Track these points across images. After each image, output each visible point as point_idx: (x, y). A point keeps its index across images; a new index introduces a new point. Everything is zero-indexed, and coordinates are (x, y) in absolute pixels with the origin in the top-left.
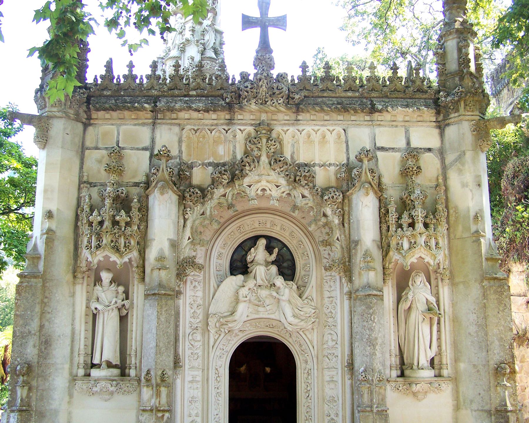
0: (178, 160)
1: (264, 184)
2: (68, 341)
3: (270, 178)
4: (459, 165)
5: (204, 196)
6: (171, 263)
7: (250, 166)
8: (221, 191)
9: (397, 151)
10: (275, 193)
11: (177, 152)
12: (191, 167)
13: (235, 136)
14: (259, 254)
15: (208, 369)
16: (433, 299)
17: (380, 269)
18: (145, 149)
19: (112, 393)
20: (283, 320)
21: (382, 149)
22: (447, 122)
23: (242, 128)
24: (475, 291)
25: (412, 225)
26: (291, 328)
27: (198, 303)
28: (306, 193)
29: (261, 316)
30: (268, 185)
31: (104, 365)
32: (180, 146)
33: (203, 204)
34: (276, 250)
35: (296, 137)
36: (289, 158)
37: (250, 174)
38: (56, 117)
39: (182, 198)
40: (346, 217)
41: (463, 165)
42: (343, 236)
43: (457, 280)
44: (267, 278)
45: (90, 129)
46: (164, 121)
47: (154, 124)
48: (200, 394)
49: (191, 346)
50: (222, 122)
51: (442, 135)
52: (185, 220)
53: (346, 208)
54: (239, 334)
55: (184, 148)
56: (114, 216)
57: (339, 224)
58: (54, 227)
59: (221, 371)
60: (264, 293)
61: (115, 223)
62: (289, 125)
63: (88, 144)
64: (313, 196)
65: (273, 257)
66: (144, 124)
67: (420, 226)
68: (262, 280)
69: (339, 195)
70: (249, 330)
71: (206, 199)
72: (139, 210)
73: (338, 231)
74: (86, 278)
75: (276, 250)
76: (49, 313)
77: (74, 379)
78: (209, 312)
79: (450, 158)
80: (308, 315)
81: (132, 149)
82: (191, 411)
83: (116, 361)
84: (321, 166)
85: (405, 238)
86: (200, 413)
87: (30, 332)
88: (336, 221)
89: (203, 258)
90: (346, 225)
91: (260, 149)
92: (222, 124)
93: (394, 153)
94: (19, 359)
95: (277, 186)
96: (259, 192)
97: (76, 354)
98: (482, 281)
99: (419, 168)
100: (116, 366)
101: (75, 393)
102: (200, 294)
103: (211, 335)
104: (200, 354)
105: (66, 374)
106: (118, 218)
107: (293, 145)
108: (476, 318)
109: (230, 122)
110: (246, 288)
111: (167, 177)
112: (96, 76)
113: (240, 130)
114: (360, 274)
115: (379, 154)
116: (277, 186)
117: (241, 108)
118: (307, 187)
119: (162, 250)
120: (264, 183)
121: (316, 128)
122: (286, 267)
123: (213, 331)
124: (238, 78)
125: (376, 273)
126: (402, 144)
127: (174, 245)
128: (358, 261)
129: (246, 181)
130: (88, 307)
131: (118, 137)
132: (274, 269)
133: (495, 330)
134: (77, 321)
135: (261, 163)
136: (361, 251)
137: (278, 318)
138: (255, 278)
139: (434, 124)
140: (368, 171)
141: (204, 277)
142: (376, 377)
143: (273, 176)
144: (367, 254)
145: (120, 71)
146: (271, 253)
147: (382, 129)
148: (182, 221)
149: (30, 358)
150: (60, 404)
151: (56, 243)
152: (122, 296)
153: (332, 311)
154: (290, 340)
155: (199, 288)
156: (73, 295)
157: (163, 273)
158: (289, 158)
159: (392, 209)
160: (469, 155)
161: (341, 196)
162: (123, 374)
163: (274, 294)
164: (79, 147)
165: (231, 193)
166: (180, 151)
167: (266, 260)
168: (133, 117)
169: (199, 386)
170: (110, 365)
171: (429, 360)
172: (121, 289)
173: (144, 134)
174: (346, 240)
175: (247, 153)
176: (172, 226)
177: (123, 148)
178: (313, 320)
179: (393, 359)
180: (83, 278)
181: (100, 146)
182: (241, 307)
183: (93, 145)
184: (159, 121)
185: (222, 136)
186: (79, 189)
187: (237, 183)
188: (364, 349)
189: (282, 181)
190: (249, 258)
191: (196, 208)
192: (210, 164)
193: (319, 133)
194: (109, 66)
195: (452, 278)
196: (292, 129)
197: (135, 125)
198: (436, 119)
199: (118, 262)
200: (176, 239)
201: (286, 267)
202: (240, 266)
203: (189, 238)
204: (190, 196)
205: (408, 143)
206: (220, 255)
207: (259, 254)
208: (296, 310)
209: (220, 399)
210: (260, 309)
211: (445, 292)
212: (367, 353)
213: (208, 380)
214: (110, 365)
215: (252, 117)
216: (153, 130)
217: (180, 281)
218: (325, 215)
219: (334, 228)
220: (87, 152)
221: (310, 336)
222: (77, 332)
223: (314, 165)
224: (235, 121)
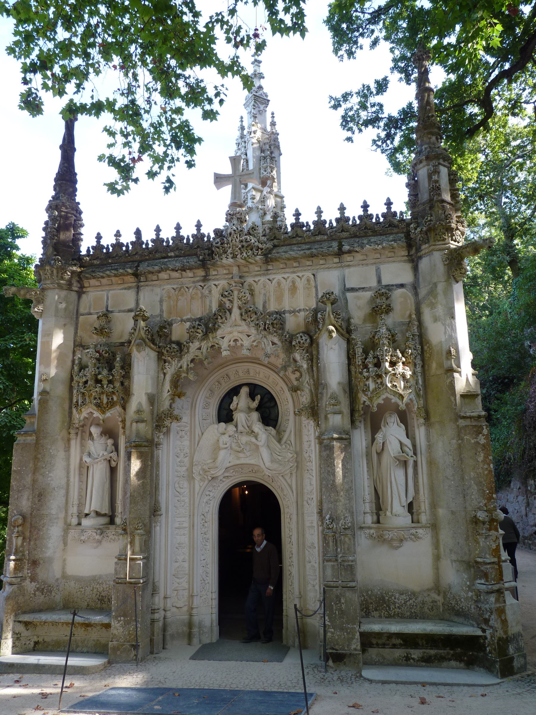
0: (159, 319)
1: (236, 335)
2: (63, 492)
3: (240, 329)
4: (431, 298)
5: (181, 350)
6: (146, 416)
7: (222, 318)
8: (197, 344)
9: (367, 291)
10: (247, 342)
11: (159, 311)
12: (170, 324)
13: (210, 291)
14: (242, 401)
15: (194, 515)
16: (407, 442)
17: (346, 411)
18: (130, 311)
19: (100, 542)
21: (352, 290)
22: (419, 254)
23: (217, 283)
24: (450, 430)
28: (276, 340)
29: (242, 461)
30: (240, 335)
31: (93, 514)
32: (161, 305)
33: (181, 358)
34: (259, 397)
35: (267, 286)
36: (261, 308)
37: (222, 326)
38: (50, 289)
39: (160, 355)
40: (315, 361)
41: (435, 297)
42: (311, 380)
43: (433, 420)
45: (84, 296)
46: (147, 283)
47: (138, 287)
48: (187, 540)
49: (177, 494)
50: (198, 278)
51: (416, 269)
52: (165, 374)
53: (314, 353)
54: (224, 480)
55: (165, 308)
56: (96, 375)
57: (308, 369)
58: (48, 389)
59: (209, 517)
60: (244, 439)
61: (98, 381)
62: (260, 275)
63: (82, 310)
64: (282, 342)
65: (255, 404)
66: (129, 288)
69: (306, 340)
71: (183, 353)
72: (122, 368)
73: (307, 376)
74: (80, 433)
76: (43, 467)
77: (67, 527)
79: (423, 291)
81: (120, 311)
82: (178, 557)
83: (105, 510)
84: (290, 312)
85: (370, 379)
86: (187, 558)
87: (25, 486)
88: (305, 366)
90: (315, 369)
91: (231, 301)
92: (198, 281)
93: (364, 293)
94: (15, 512)
95: (249, 336)
96: (232, 343)
97: (70, 505)
98: (456, 421)
99: (389, 306)
100: (105, 515)
101: (69, 541)
102: (187, 443)
103: (196, 482)
104: (187, 500)
105: (61, 524)
106: (99, 377)
107: (265, 295)
108: (452, 461)
109: (205, 279)
110: (226, 436)
111: (144, 336)
112: (89, 248)
113: (215, 285)
114: (326, 418)
115: (349, 295)
116: (249, 336)
117: (214, 265)
118: (275, 334)
119: (140, 404)
120: (235, 333)
121: (286, 276)
122: (268, 412)
123: (197, 478)
124: (212, 235)
125: (343, 417)
126: (374, 283)
127: (152, 399)
128: (324, 405)
129: (219, 333)
130: (81, 459)
131: (107, 302)
132: (255, 415)
133: (472, 473)
134: (72, 473)
135: (232, 314)
136: (327, 394)
138: (236, 426)
139: (406, 258)
140: (331, 313)
141: (191, 428)
142: (340, 525)
143: (244, 327)
144: (334, 397)
145: (108, 240)
146: (253, 400)
147: (352, 269)
148: (162, 375)
149: (25, 510)
150: (55, 552)
151: (51, 403)
152: (111, 447)
154: (273, 484)
155: (186, 437)
156: (67, 449)
157: (142, 426)
158: (261, 308)
159: (359, 351)
160: (441, 287)
161: (308, 340)
162: (112, 522)
163: (253, 440)
164: (73, 314)
165: (206, 346)
166: (162, 311)
167: (249, 408)
168: (119, 282)
169: (186, 532)
170: (98, 514)
171: (405, 504)
172: (110, 442)
173: (128, 298)
174: (314, 385)
175: (221, 306)
176: (150, 382)
177: (112, 312)
178: (292, 465)
179: (367, 505)
180: (77, 434)
181: (92, 311)
182: (222, 454)
183: (86, 311)
184: (142, 284)
185: (199, 292)
186: (74, 352)
187: (210, 335)
188: (329, 496)
189: (253, 331)
190: (232, 407)
191: (173, 363)
192: (188, 320)
193: (289, 280)
194: (99, 237)
195: (427, 418)
196: (263, 279)
197: (122, 289)
198: (409, 253)
199: (101, 418)
200: (154, 392)
203: (169, 391)
204: (167, 351)
205: (379, 281)
207: (242, 401)
209: (207, 544)
210: (241, 455)
211: (421, 433)
212: (332, 500)
213: (193, 526)
214: (98, 514)
215: (225, 272)
216: (138, 293)
217: (160, 432)
218: (295, 361)
219: (303, 373)
220: (81, 318)
221: (289, 481)
222: (71, 484)
223: (284, 312)
224: (210, 277)
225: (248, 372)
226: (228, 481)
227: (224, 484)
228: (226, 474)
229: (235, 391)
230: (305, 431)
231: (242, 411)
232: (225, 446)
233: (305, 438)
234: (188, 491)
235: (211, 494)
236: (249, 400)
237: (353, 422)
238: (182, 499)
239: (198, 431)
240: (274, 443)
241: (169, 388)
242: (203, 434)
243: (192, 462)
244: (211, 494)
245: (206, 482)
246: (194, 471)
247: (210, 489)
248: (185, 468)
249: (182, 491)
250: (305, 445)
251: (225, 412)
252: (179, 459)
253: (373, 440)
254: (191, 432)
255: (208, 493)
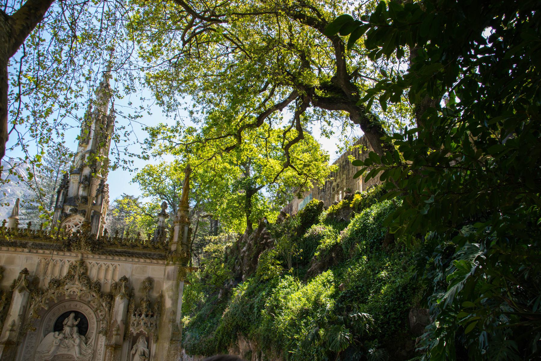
14: (70, 320)
25: (140, 315)
65: (76, 323)
67: (143, 316)
91: (75, 272)
96: (72, 293)
132: (75, 329)
187: (61, 288)
201: (83, 328)
202: (58, 327)
206: (50, 320)
225: (76, 305)
229: (66, 315)
230: (100, 340)
231: (69, 326)
233: (99, 343)
236: (74, 321)
237: (124, 339)
240: (84, 346)
250: (99, 347)
253: (132, 348)
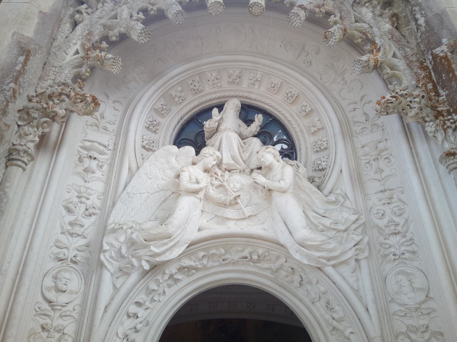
20: (284, 238)
26: (306, 256)
27: (89, 202)
29: (232, 227)
34: (259, 119)
44: (245, 158)
49: (45, 306)
52: (75, 24)
54: (179, 276)
68: (233, 158)
70: (205, 268)
75: (259, 119)
78: (110, 221)
80: (343, 228)
89: (117, 123)
103: (107, 276)
123: (111, 266)
137: (269, 234)
141: (113, 158)
153: (397, 219)
155: (98, 174)
182: (186, 204)
190: (208, 125)
203: (77, 52)
208: (311, 215)
210: (230, 213)
226: (186, 280)
227: (175, 288)
228: (187, 262)
232: (196, 186)
234: (78, 301)
235: (141, 312)
238: (58, 322)
239: (129, 160)
241: (78, 47)
242: (138, 168)
243: (105, 227)
244: (141, 312)
245: (134, 277)
246: (106, 247)
247: (142, 297)
248: (82, 242)
249: (63, 298)
251: (190, 134)
252: (71, 218)
254: (111, 165)
255: (133, 309)
